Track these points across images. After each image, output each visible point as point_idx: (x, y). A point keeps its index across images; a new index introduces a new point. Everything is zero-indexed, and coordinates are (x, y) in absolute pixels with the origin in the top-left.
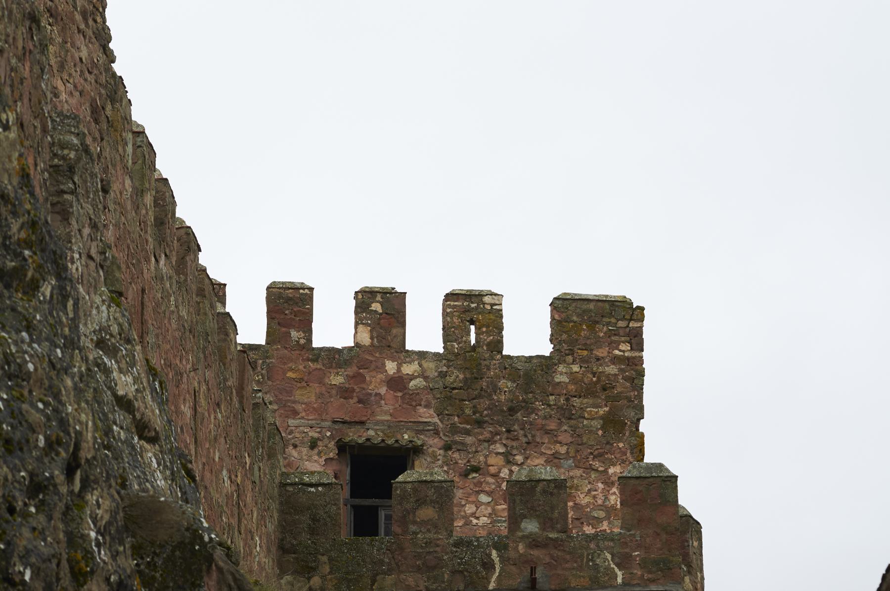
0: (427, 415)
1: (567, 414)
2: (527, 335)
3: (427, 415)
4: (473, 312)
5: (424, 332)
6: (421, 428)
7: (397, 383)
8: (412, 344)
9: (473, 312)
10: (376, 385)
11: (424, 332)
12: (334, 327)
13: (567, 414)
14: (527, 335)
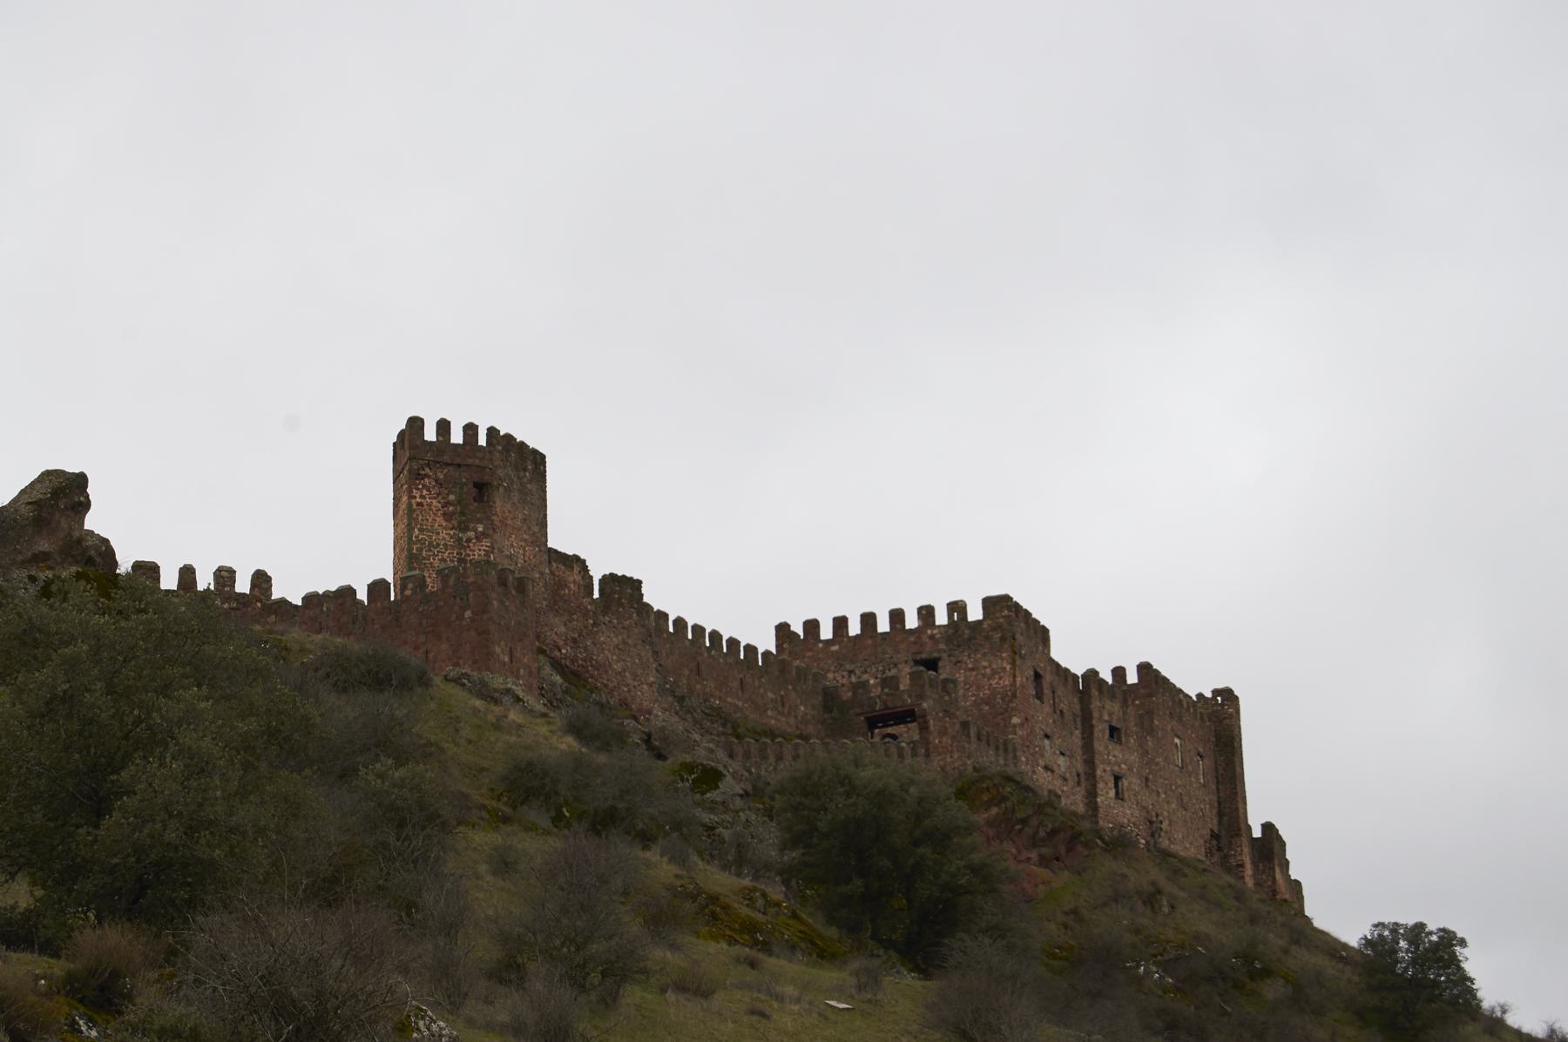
0: (942, 646)
1: (987, 638)
2: (975, 613)
3: (942, 646)
4: (957, 608)
5: (941, 618)
6: (940, 651)
7: (932, 637)
8: (938, 623)
9: (957, 608)
10: (925, 639)
11: (941, 618)
12: (912, 622)
13: (987, 638)
14: (975, 613)
